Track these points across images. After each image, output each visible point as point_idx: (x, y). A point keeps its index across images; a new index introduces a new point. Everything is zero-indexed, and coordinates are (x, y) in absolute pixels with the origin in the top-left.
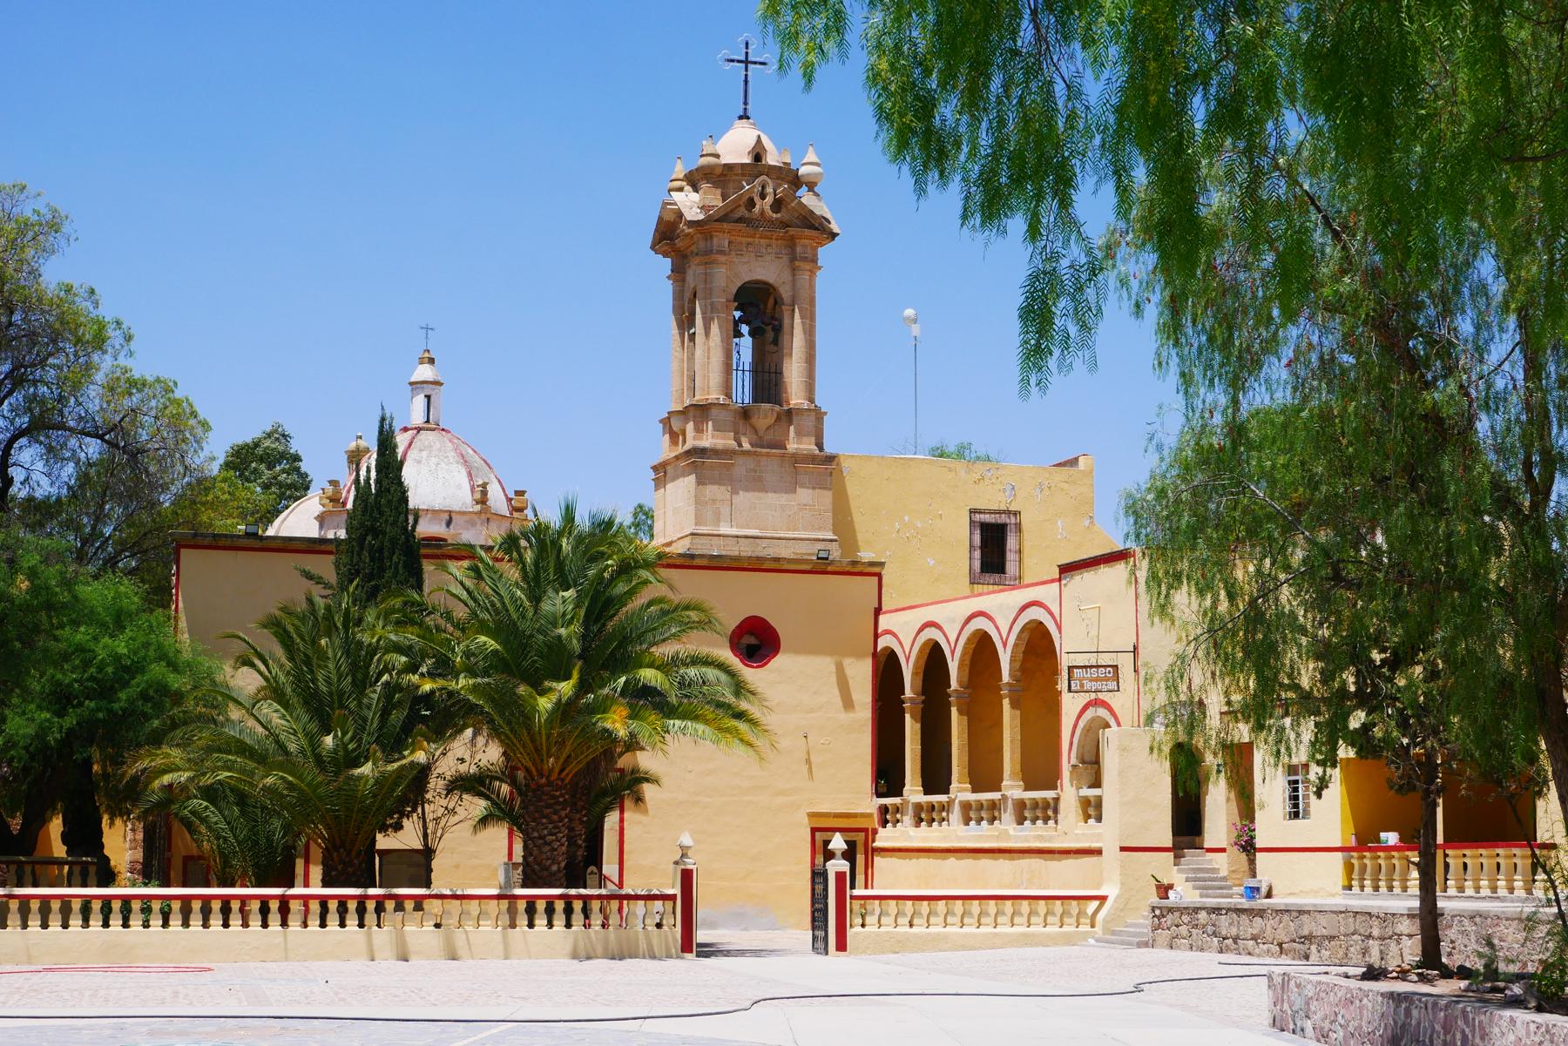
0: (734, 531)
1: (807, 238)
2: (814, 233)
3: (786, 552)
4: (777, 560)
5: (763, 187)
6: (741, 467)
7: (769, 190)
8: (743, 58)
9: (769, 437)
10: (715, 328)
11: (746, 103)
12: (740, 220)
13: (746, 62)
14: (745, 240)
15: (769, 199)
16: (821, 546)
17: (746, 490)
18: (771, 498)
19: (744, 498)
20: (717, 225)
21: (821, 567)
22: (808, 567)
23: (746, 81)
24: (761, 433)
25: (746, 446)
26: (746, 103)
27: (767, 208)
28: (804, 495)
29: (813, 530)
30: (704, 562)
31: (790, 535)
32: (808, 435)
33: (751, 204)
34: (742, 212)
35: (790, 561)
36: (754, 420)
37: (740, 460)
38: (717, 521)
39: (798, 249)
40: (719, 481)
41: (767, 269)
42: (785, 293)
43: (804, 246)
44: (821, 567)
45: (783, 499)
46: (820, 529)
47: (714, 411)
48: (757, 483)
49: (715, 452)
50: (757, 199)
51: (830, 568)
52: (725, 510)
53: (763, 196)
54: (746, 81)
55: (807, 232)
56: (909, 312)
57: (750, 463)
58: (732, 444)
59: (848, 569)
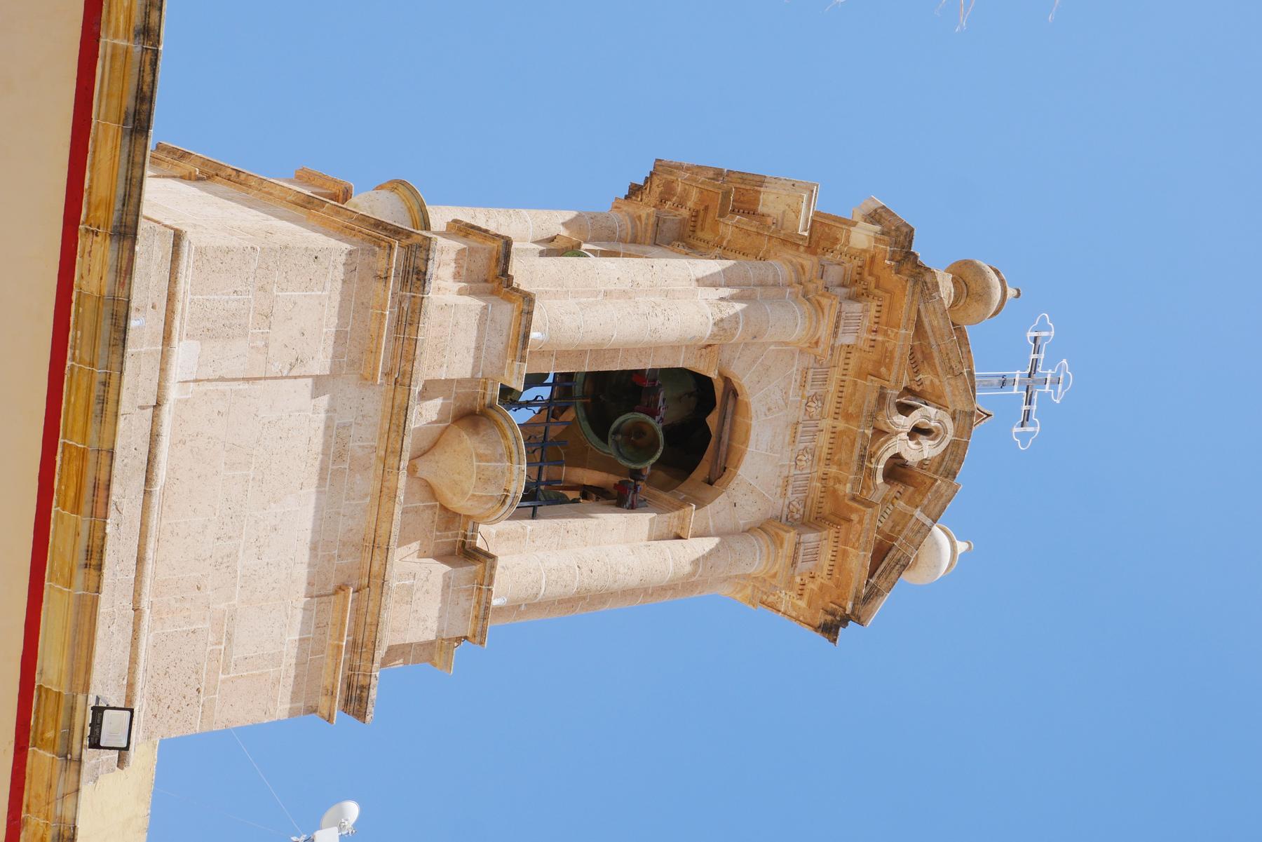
1: (840, 557)
4: (94, 559)
7: (927, 450)
14: (832, 387)
20: (905, 307)
22: (51, 669)
24: (426, 469)
31: (145, 604)
35: (87, 611)
36: (467, 443)
38: (207, 334)
39: (811, 537)
41: (768, 453)
42: (718, 509)
43: (815, 555)
47: (506, 312)
49: (409, 318)
51: (41, 759)
53: (918, 432)
55: (859, 561)
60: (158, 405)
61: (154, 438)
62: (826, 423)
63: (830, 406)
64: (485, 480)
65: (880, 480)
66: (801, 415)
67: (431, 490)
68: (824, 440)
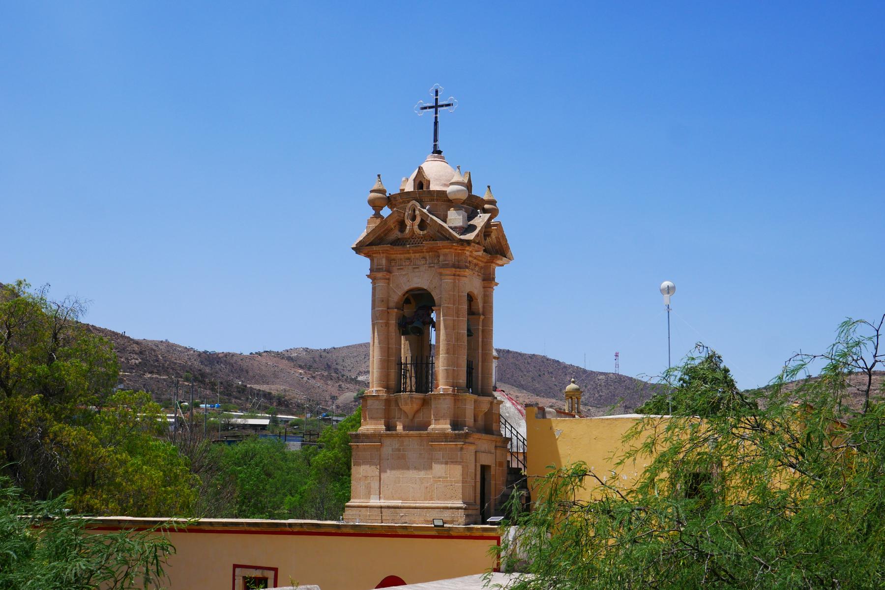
0: (383, 503)
1: (444, 247)
2: (446, 243)
3: (418, 522)
5: (414, 211)
6: (389, 447)
8: (440, 103)
9: (420, 418)
10: (376, 334)
11: (435, 140)
12: (397, 242)
13: (436, 107)
14: (402, 256)
15: (418, 220)
16: (447, 515)
17: (393, 468)
18: (412, 474)
19: (389, 476)
21: (442, 533)
23: (436, 123)
25: (400, 428)
26: (435, 140)
27: (416, 227)
28: (439, 469)
29: (446, 499)
30: (352, 531)
32: (444, 417)
33: (402, 225)
34: (396, 234)
37: (387, 442)
38: (368, 496)
39: (441, 258)
40: (370, 463)
43: (445, 255)
44: (442, 533)
45: (422, 474)
46: (451, 498)
48: (401, 462)
50: (408, 222)
51: (453, 533)
52: (375, 485)
53: (414, 218)
54: (436, 123)
56: (666, 284)
57: (395, 444)
58: (382, 427)
59: (468, 534)
60: (381, 507)
61: (389, 507)
62: (413, 255)
63: (407, 256)
64: (406, 404)
65: (425, 232)
66: (410, 267)
67: (417, 411)
68: (417, 255)
